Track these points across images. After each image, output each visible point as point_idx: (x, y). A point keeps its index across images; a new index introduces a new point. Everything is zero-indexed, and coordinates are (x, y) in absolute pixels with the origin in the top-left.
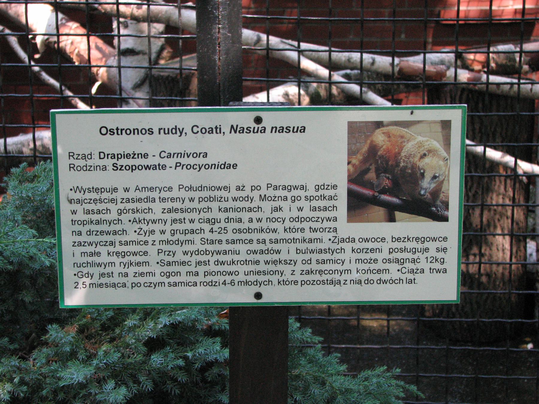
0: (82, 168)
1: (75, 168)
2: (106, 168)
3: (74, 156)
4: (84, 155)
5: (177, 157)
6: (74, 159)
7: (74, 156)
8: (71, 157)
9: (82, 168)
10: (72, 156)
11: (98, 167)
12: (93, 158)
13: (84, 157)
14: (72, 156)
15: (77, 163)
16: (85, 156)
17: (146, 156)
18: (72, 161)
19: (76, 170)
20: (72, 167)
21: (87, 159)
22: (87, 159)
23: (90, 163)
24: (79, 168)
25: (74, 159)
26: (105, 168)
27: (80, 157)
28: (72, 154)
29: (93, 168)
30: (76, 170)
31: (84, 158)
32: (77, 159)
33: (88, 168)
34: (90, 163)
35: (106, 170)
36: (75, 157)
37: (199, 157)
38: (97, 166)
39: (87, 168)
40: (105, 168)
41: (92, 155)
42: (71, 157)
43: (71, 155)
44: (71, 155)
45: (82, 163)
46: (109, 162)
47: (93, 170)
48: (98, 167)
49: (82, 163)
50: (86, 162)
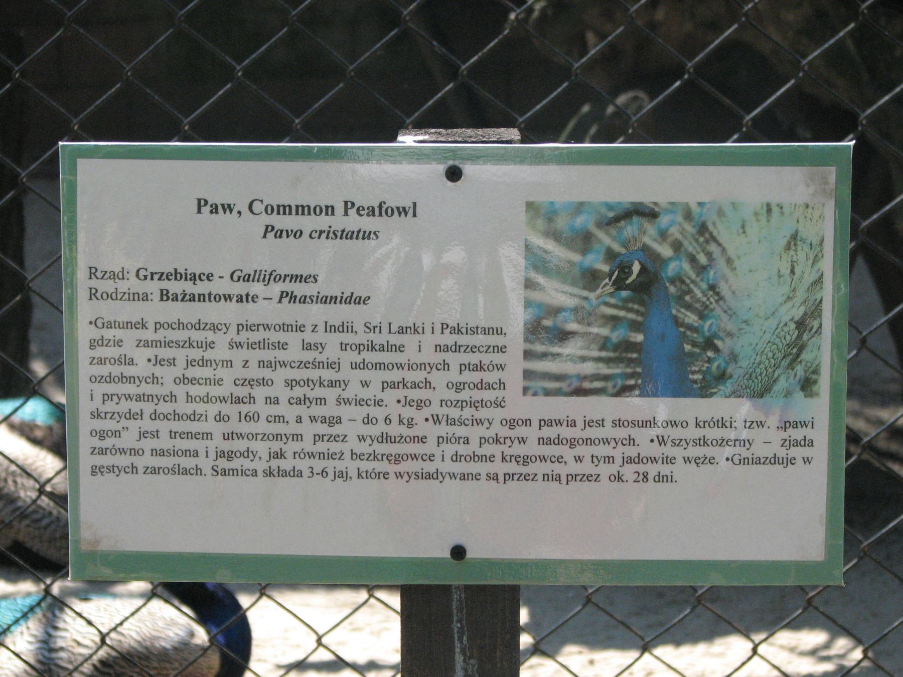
3: (96, 274)
5: (290, 281)
6: (97, 278)
7: (96, 274)
13: (114, 276)
16: (114, 275)
17: (209, 277)
18: (94, 283)
20: (93, 294)
23: (123, 286)
26: (146, 297)
34: (123, 286)
37: (284, 281)
40: (146, 297)
41: (125, 272)
43: (93, 272)
44: (93, 272)
45: (107, 286)
46: (153, 287)
49: (107, 286)
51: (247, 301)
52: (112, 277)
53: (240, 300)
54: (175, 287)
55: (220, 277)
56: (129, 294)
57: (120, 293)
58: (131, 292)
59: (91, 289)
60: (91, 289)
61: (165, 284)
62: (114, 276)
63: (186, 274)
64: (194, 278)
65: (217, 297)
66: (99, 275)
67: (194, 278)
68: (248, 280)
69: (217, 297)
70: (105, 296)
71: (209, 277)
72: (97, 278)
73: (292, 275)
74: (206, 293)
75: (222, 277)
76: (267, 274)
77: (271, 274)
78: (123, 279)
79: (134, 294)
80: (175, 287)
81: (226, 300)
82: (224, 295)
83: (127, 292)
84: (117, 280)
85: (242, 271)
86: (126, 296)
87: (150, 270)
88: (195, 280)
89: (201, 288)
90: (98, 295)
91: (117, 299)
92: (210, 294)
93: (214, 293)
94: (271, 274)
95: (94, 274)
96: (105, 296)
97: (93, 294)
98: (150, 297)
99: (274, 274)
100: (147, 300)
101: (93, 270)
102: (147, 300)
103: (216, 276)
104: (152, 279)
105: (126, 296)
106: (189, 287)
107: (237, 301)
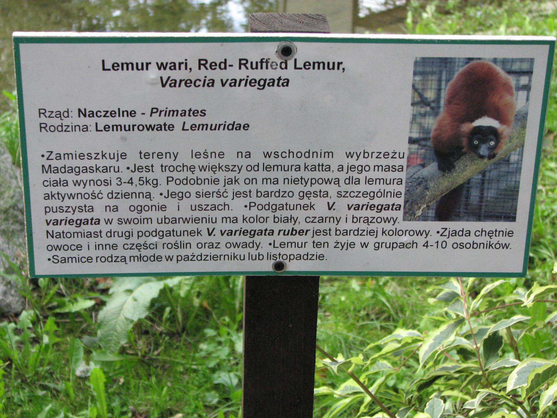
0: (56, 129)
1: (47, 128)
2: (87, 128)
3: (45, 114)
4: (59, 113)
6: (46, 117)
7: (45, 114)
8: (42, 115)
9: (56, 129)
10: (43, 113)
11: (77, 128)
12: (70, 116)
13: (59, 115)
14: (43, 113)
15: (49, 122)
16: (60, 114)
18: (43, 119)
19: (48, 130)
20: (43, 127)
21: (63, 118)
22: (63, 118)
23: (66, 122)
24: (52, 129)
25: (46, 117)
26: (86, 129)
27: (53, 115)
28: (43, 111)
29: (70, 129)
30: (48, 130)
31: (58, 116)
32: (49, 117)
33: (64, 128)
34: (66, 122)
35: (87, 130)
36: (48, 114)
38: (75, 126)
40: (86, 129)
42: (42, 115)
44: (42, 112)
45: (56, 122)
47: (71, 130)
48: (77, 128)
49: (56, 122)
56: (72, 126)
57: (65, 126)
98: (89, 129)
106: (117, 120)
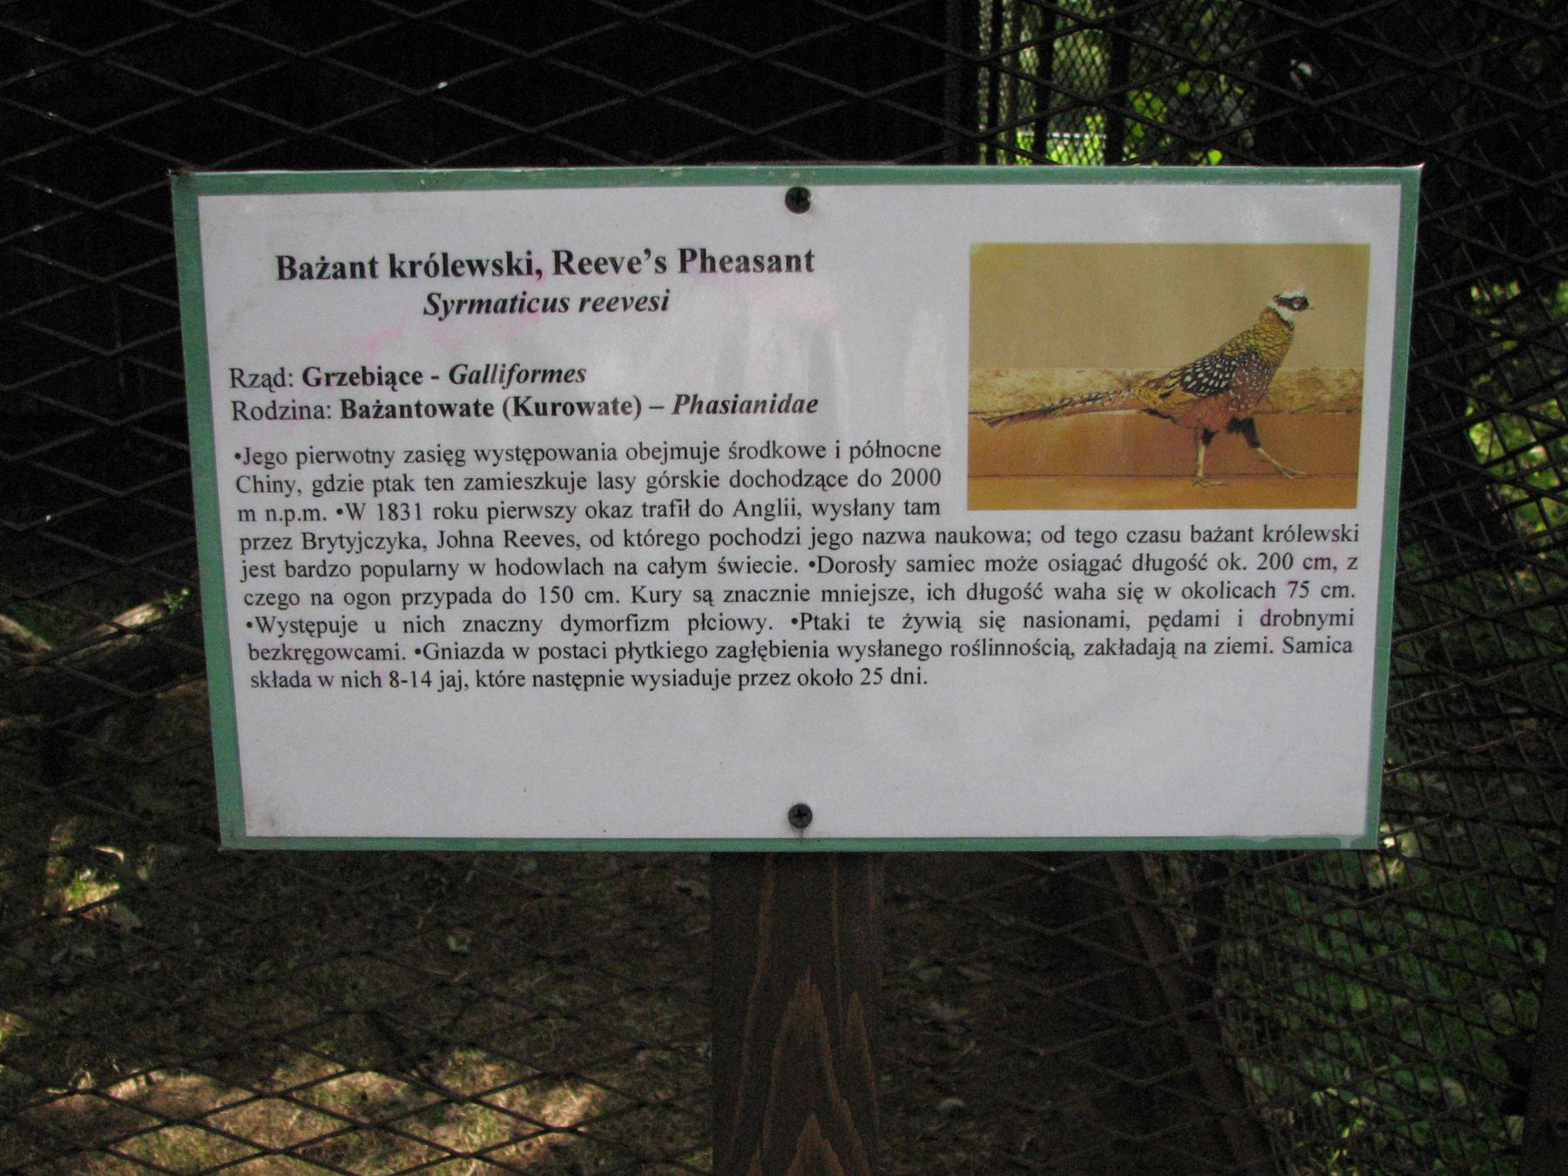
5: (543, 380)
6: (243, 385)
13: (270, 382)
17: (416, 378)
18: (240, 394)
20: (239, 410)
23: (283, 397)
30: (249, 416)
34: (283, 397)
37: (533, 380)
39: (272, 413)
40: (320, 413)
41: (286, 377)
43: (236, 377)
44: (236, 377)
45: (259, 398)
46: (331, 397)
50: (273, 396)
51: (477, 414)
52: (267, 383)
53: (466, 411)
54: (365, 395)
55: (433, 378)
58: (297, 405)
59: (235, 403)
60: (235, 403)
61: (348, 392)
62: (270, 382)
63: (380, 374)
64: (392, 380)
65: (431, 409)
66: (247, 380)
67: (392, 380)
68: (477, 381)
69: (431, 409)
70: (257, 413)
71: (416, 378)
72: (243, 385)
73: (545, 371)
74: (413, 404)
75: (433, 378)
76: (508, 368)
77: (512, 371)
78: (283, 385)
79: (301, 408)
80: (365, 395)
81: (444, 414)
82: (441, 406)
83: (291, 405)
84: (274, 388)
85: (466, 366)
86: (290, 412)
87: (325, 370)
88: (394, 382)
89: (406, 395)
90: (247, 412)
91: (275, 418)
92: (418, 405)
93: (424, 403)
94: (512, 371)
95: (239, 379)
96: (257, 413)
97: (239, 410)
98: (326, 414)
99: (518, 370)
100: (322, 417)
101: (237, 374)
102: (322, 417)
103: (426, 380)
104: (328, 383)
105: (290, 412)
106: (386, 395)
107: (462, 414)
